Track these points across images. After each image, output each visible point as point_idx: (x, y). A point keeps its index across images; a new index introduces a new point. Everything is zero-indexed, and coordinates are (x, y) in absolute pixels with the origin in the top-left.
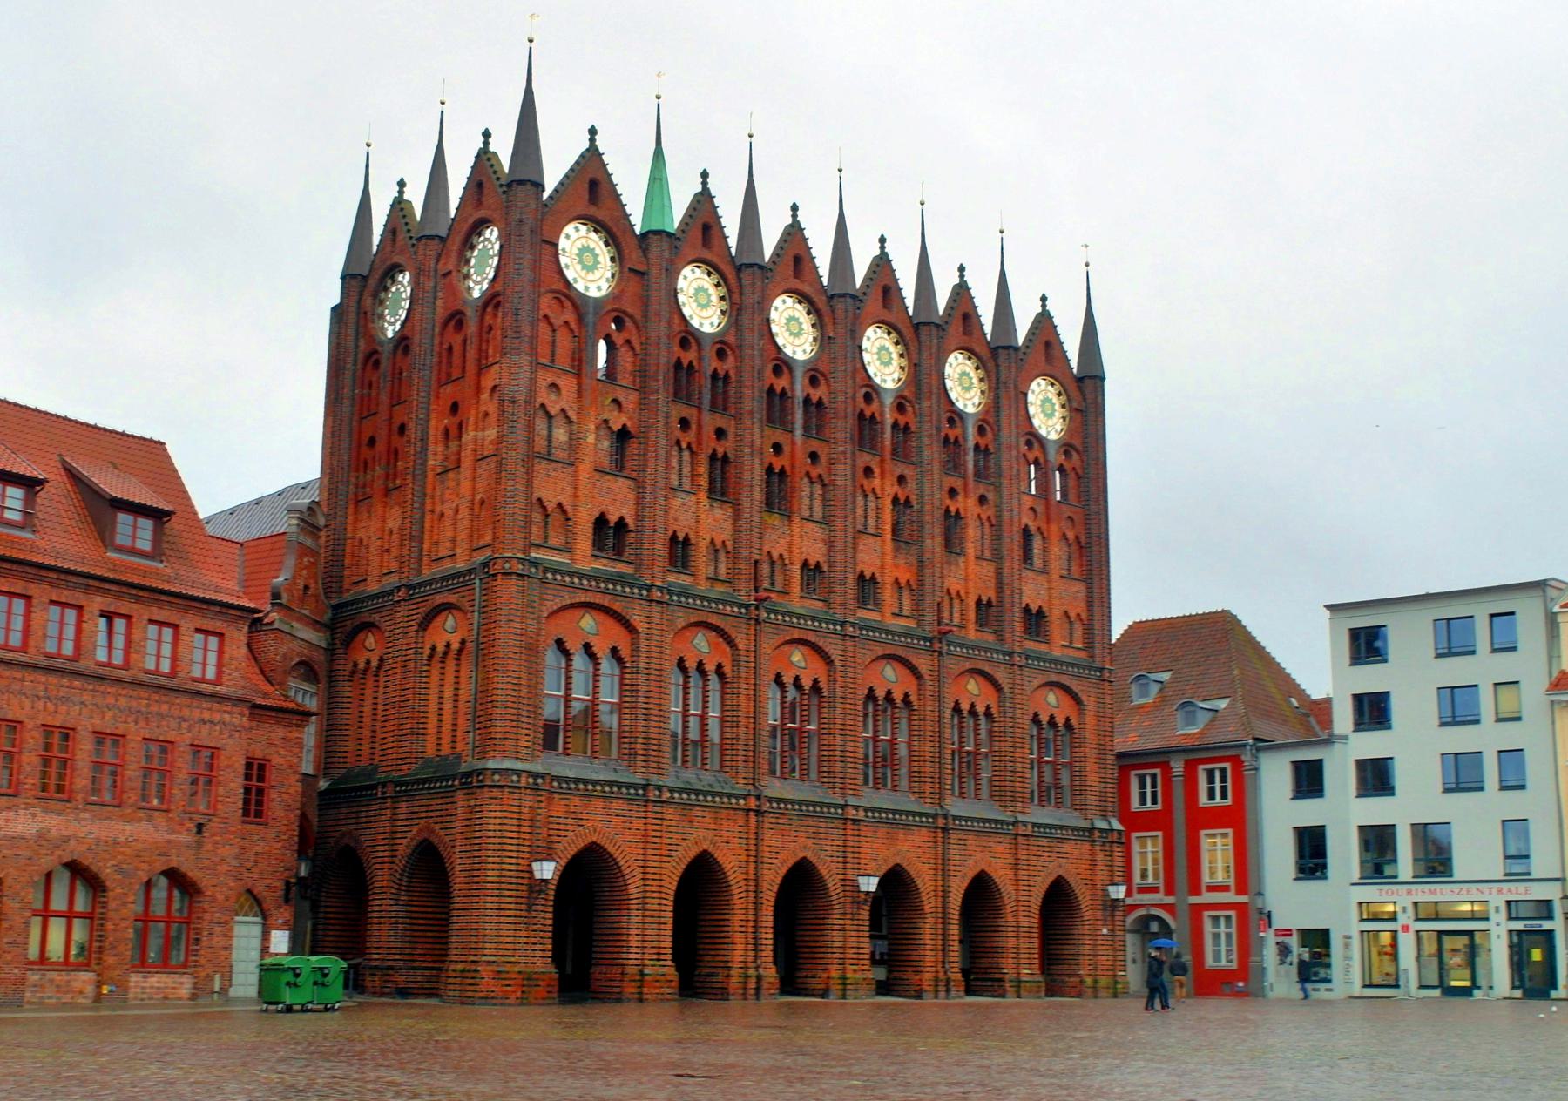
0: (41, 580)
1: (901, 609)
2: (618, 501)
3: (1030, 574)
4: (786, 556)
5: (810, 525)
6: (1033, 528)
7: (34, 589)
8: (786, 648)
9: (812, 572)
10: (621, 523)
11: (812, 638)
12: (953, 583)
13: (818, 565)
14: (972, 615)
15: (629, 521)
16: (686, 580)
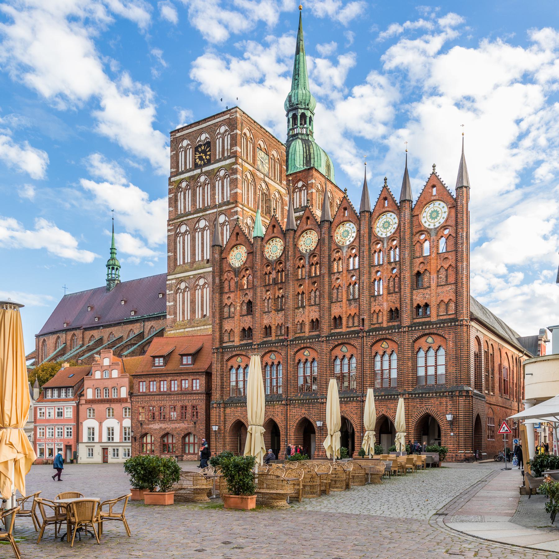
0: (157, 377)
1: (353, 323)
2: (247, 322)
3: (422, 291)
4: (304, 320)
5: (313, 307)
6: (422, 272)
7: (156, 379)
8: (302, 351)
9: (315, 324)
10: (250, 329)
11: (308, 345)
12: (377, 308)
13: (317, 319)
14: (385, 318)
15: (251, 327)
16: (270, 339)
